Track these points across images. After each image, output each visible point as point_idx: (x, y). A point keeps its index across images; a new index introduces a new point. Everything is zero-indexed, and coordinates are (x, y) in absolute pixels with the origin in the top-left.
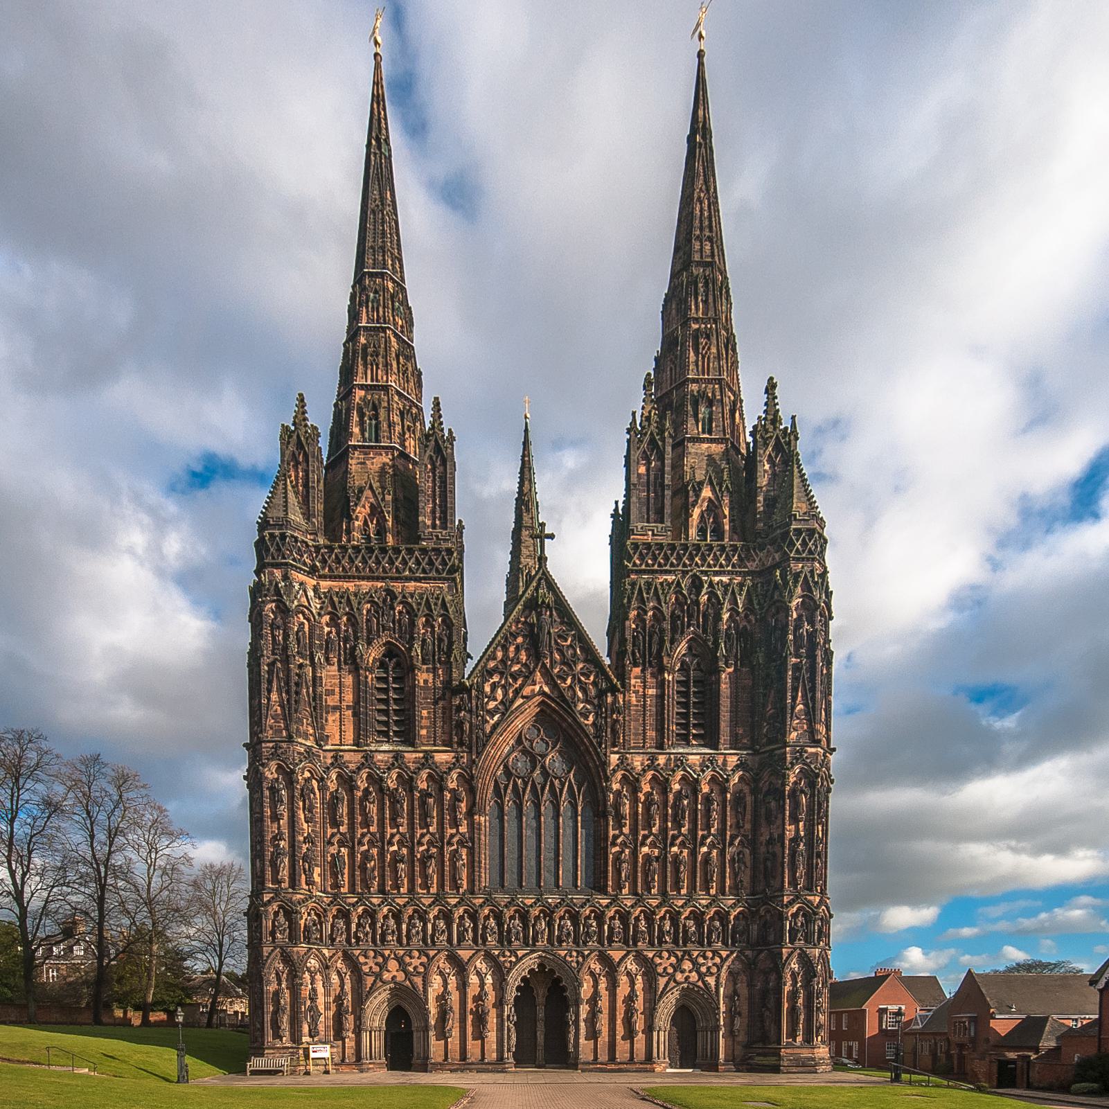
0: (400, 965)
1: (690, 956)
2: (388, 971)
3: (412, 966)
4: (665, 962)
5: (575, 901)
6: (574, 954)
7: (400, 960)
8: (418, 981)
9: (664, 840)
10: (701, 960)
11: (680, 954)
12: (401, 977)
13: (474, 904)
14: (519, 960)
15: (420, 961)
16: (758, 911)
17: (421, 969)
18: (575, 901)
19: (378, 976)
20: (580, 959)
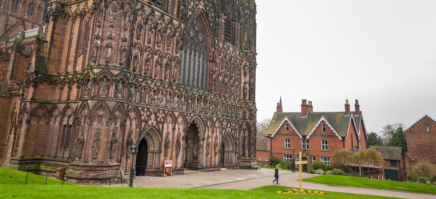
0: (155, 117)
1: (230, 121)
2: (151, 120)
4: (225, 123)
7: (155, 114)
8: (161, 126)
9: (225, 76)
10: (231, 124)
12: (155, 123)
14: (192, 118)
15: (162, 116)
16: (243, 106)
17: (162, 120)
19: (147, 122)
20: (206, 120)
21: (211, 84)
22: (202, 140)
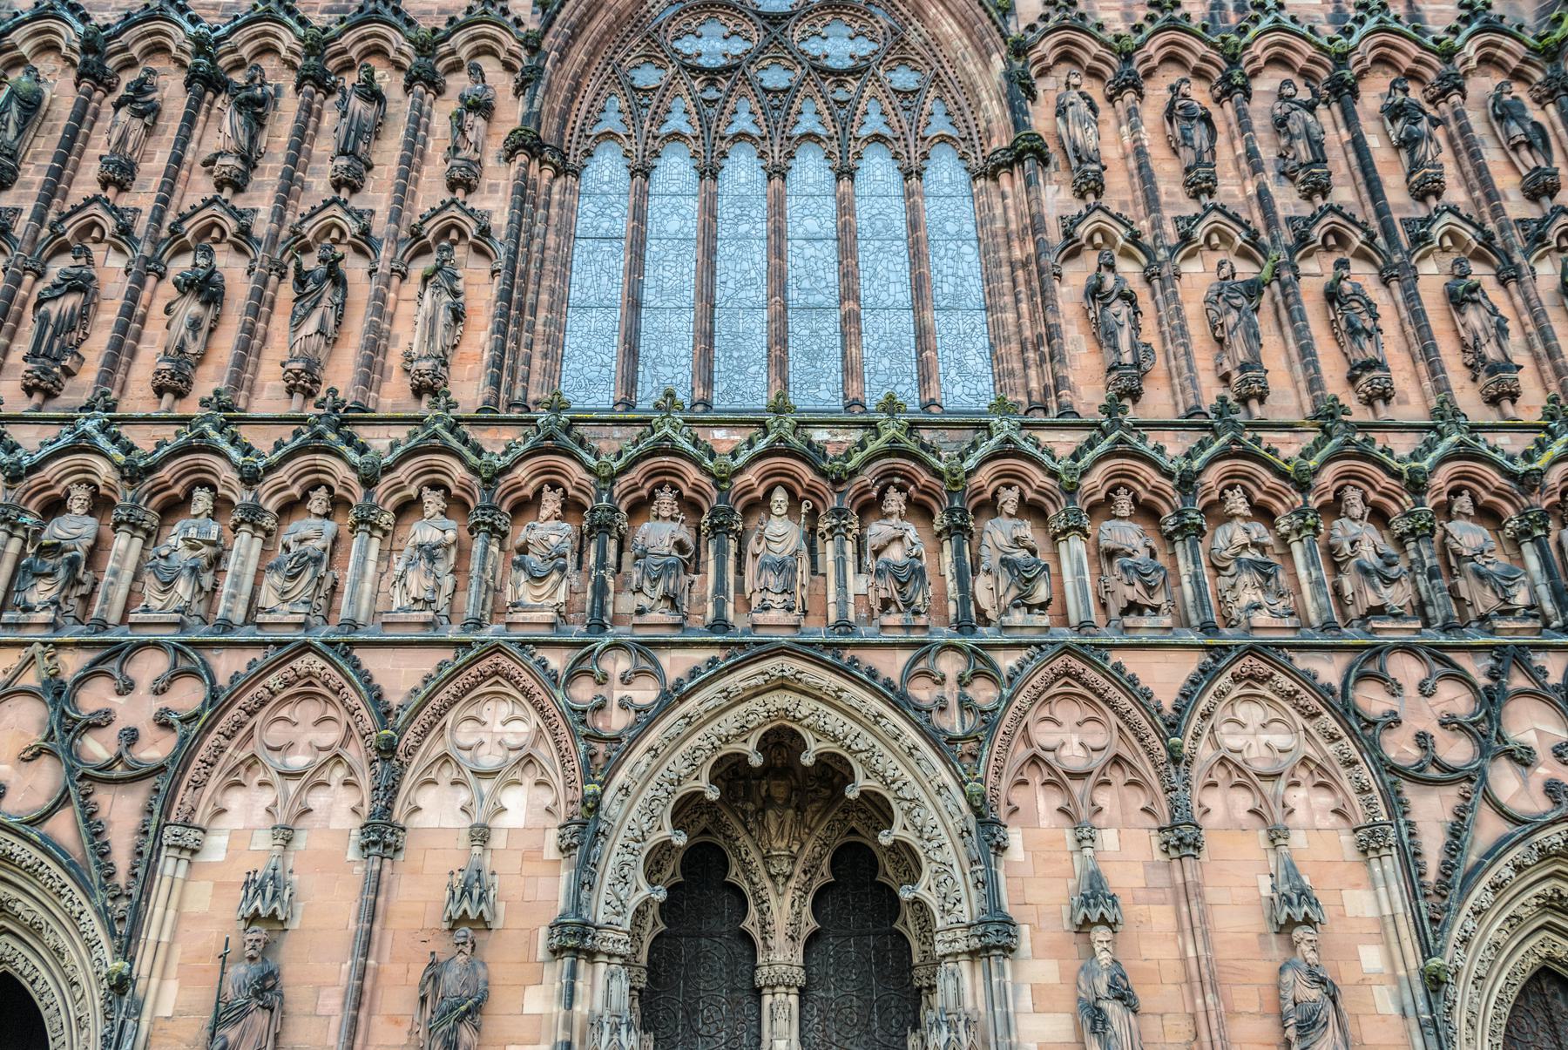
3: (111, 733)
5: (927, 436)
6: (950, 666)
11: (1476, 668)
13: (478, 451)
14: (671, 697)
18: (927, 436)
21: (1036, 347)
22: (973, 954)
